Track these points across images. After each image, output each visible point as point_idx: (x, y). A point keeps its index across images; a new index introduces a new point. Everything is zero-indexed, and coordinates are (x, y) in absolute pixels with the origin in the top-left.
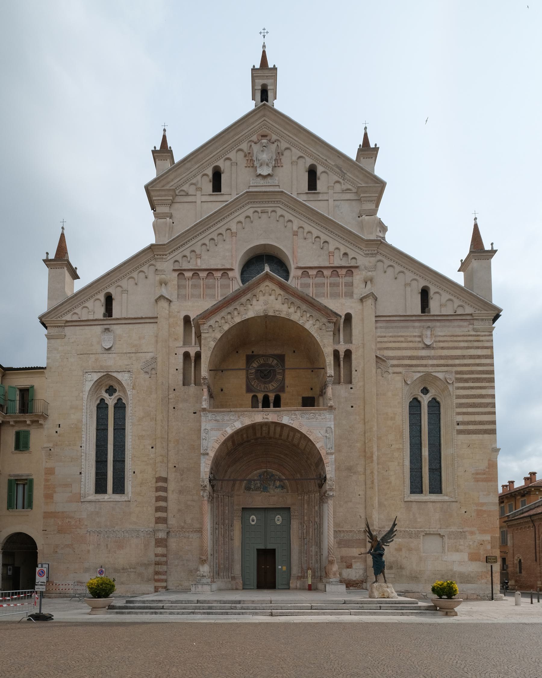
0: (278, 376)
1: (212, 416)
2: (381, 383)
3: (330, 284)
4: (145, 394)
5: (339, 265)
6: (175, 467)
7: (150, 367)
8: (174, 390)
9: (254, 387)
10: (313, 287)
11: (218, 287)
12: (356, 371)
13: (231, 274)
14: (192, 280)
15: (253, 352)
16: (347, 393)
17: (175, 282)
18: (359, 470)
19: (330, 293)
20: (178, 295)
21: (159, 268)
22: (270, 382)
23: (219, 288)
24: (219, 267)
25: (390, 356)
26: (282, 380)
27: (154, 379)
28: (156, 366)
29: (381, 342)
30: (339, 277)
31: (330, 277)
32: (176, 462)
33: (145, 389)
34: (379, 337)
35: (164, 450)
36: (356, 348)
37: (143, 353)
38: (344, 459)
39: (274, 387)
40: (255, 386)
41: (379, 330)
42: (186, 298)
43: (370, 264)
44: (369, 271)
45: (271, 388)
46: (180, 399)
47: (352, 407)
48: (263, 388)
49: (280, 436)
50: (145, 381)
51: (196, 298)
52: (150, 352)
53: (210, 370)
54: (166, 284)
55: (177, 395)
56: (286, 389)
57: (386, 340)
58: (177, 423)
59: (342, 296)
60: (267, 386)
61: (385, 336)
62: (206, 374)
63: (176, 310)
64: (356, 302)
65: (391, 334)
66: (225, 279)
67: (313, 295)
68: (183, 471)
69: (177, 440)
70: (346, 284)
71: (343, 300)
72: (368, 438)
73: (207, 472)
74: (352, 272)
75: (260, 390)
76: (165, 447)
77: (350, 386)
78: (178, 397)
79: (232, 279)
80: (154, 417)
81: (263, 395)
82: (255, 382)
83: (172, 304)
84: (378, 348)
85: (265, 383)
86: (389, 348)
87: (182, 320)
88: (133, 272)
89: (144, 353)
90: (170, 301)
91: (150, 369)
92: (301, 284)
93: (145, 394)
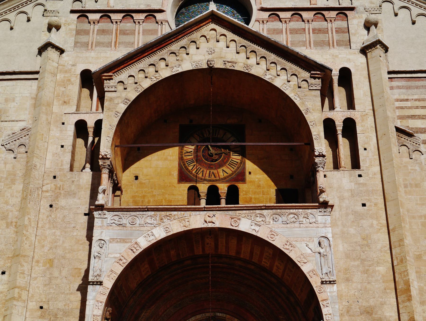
0: (232, 157)
1: (114, 217)
2: (410, 168)
3: (314, 30)
4: (3, 184)
5: (326, 6)
6: (41, 308)
7: (18, 143)
8: (55, 177)
9: (191, 173)
10: (286, 33)
11: (139, 33)
12: (365, 149)
13: (159, 16)
14: (99, 24)
15: (191, 121)
16: (353, 184)
17: (73, 27)
18: (388, 314)
19: (314, 41)
20: (76, 43)
21: (48, 9)
22: (220, 166)
23: (141, 34)
24: (143, 7)
25: (419, 128)
26: (241, 163)
27: (22, 160)
28: (28, 141)
29: (402, 108)
30: (326, 21)
31: (312, 21)
32: (44, 300)
33: (5, 176)
34: (397, 100)
35: (25, 278)
36: (361, 116)
37: (9, 121)
38: (356, 293)
39: (226, 175)
40: (194, 172)
41: (396, 91)
42: (88, 47)
43: (373, 5)
44: (372, 14)
45: (222, 175)
46: (62, 192)
47: (364, 205)
48: (207, 175)
49: (238, 252)
50: (5, 163)
51: (104, 46)
52: (20, 121)
53: (116, 146)
54: (58, 28)
55: (59, 186)
56: (248, 177)
57: (410, 106)
58: (54, 231)
59: (333, 46)
60: (215, 171)
61: (408, 99)
62: (108, 151)
63: (71, 63)
64: (355, 53)
65: (416, 97)
66: (151, 23)
67: (287, 42)
68: (56, 315)
69: (50, 260)
70: (336, 29)
71: (335, 51)
72: (397, 258)
73: (97, 316)
74: (346, 16)
75: (203, 178)
76: (26, 272)
77: (357, 172)
78: (60, 189)
79: (162, 23)
80: (14, 220)
81: (207, 187)
82: (194, 165)
83: (64, 55)
84: (398, 116)
85: (210, 167)
86: (416, 116)
87: (79, 77)
88: (8, 12)
89: (10, 122)
90: (62, 51)
91: (18, 145)
92: (269, 30)
93: (3, 184)
